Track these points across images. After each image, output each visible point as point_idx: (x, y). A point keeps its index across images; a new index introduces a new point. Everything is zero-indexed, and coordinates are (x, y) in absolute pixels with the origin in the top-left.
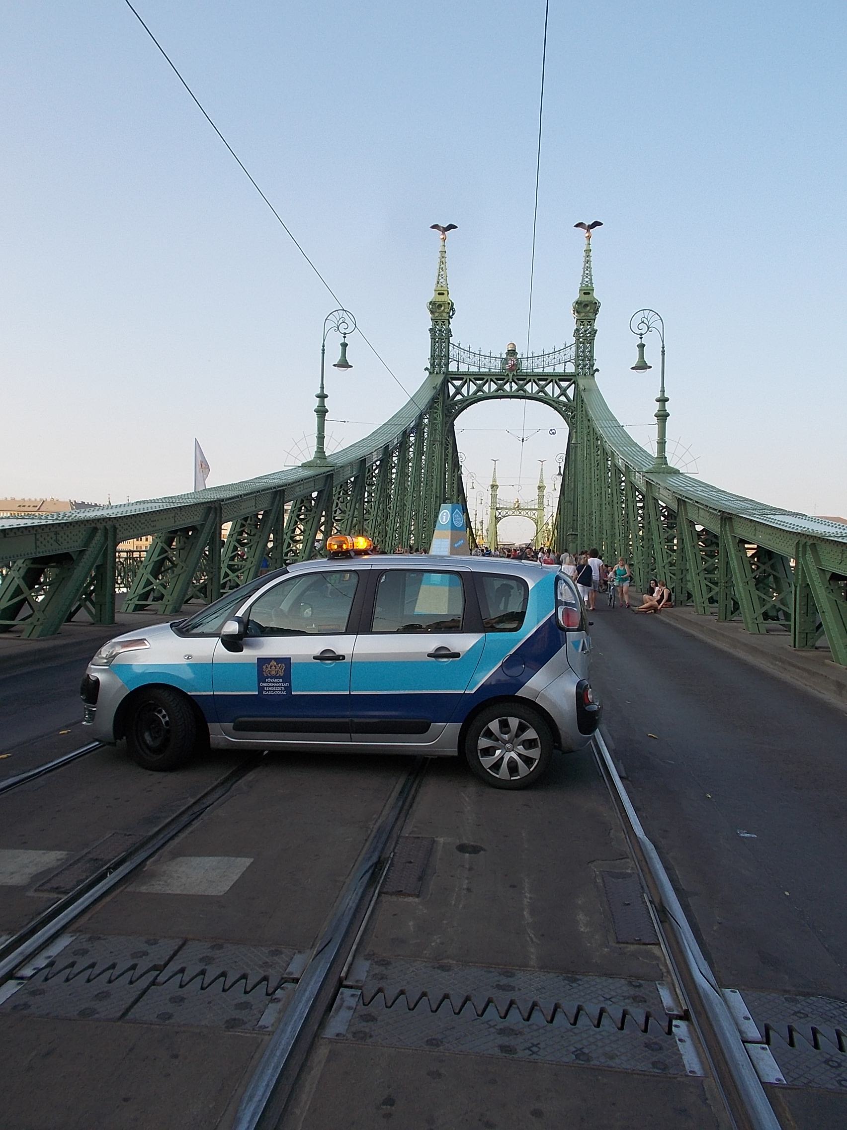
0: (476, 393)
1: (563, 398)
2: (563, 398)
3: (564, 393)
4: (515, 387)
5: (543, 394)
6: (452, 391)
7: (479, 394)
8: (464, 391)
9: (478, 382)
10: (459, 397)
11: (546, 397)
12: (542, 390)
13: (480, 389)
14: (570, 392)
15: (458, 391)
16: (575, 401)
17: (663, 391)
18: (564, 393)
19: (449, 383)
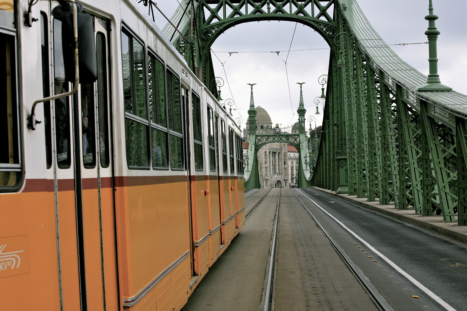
0: (232, 15)
1: (323, 18)
2: (323, 18)
3: (323, 12)
4: (273, 8)
5: (302, 15)
6: (207, 14)
7: (236, 16)
8: (220, 14)
9: (234, 4)
10: (215, 21)
11: (305, 17)
12: (301, 10)
13: (236, 11)
14: (330, 11)
15: (214, 15)
16: (336, 23)
17: (431, 10)
18: (323, 12)
19: (205, 8)
